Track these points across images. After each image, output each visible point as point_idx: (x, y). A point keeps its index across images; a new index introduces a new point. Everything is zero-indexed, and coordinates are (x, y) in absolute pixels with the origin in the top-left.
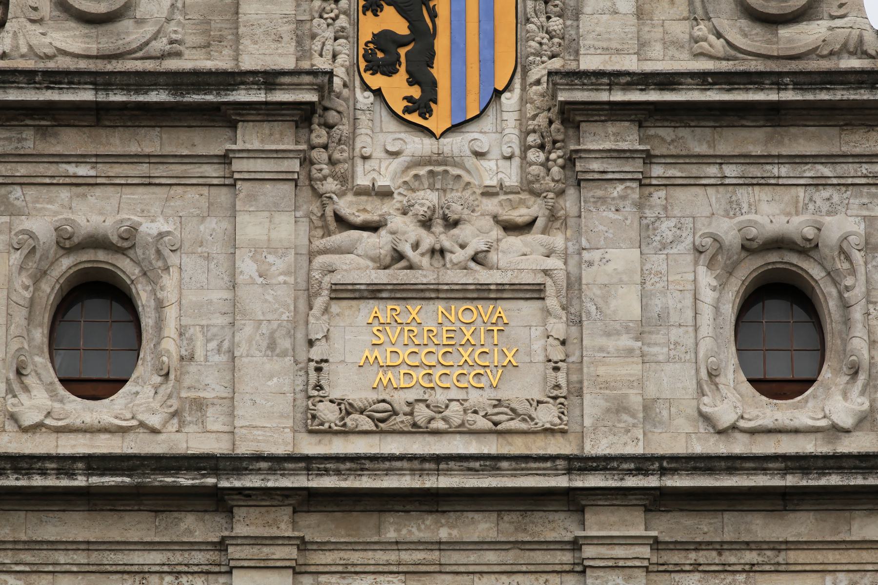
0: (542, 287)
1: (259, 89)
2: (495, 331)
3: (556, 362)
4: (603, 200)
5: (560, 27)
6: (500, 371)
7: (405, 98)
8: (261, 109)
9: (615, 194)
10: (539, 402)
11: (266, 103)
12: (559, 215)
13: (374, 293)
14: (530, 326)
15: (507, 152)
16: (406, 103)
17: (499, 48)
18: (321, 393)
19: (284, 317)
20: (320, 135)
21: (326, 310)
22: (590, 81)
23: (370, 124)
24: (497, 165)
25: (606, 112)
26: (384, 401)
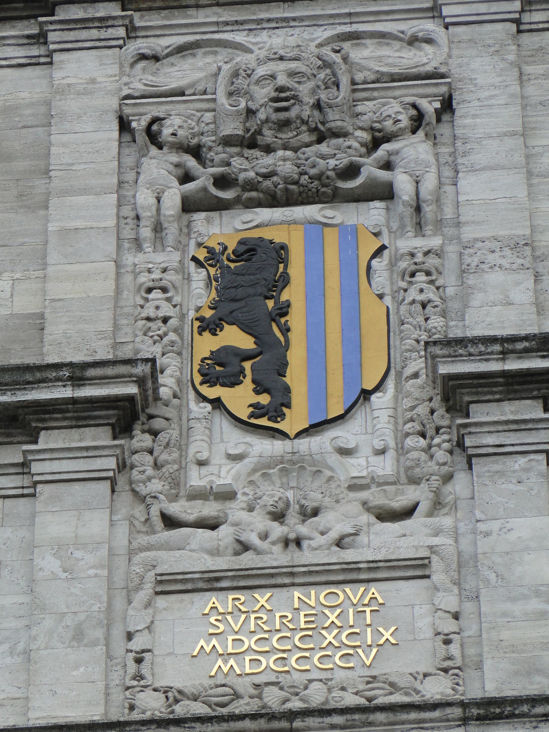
0: (426, 561)
1: (64, 386)
2: (368, 613)
3: (447, 635)
4: (501, 473)
5: (442, 324)
6: (375, 650)
7: (251, 406)
8: (68, 411)
9: (517, 467)
10: (425, 675)
11: (74, 401)
12: (447, 501)
13: (211, 582)
14: (413, 606)
15: (379, 445)
16: (251, 409)
17: (367, 354)
18: (142, 683)
19: (95, 608)
20: (141, 440)
21: (148, 605)
22: (477, 350)
23: (207, 431)
24: (367, 461)
25: (501, 388)
26: (224, 685)
